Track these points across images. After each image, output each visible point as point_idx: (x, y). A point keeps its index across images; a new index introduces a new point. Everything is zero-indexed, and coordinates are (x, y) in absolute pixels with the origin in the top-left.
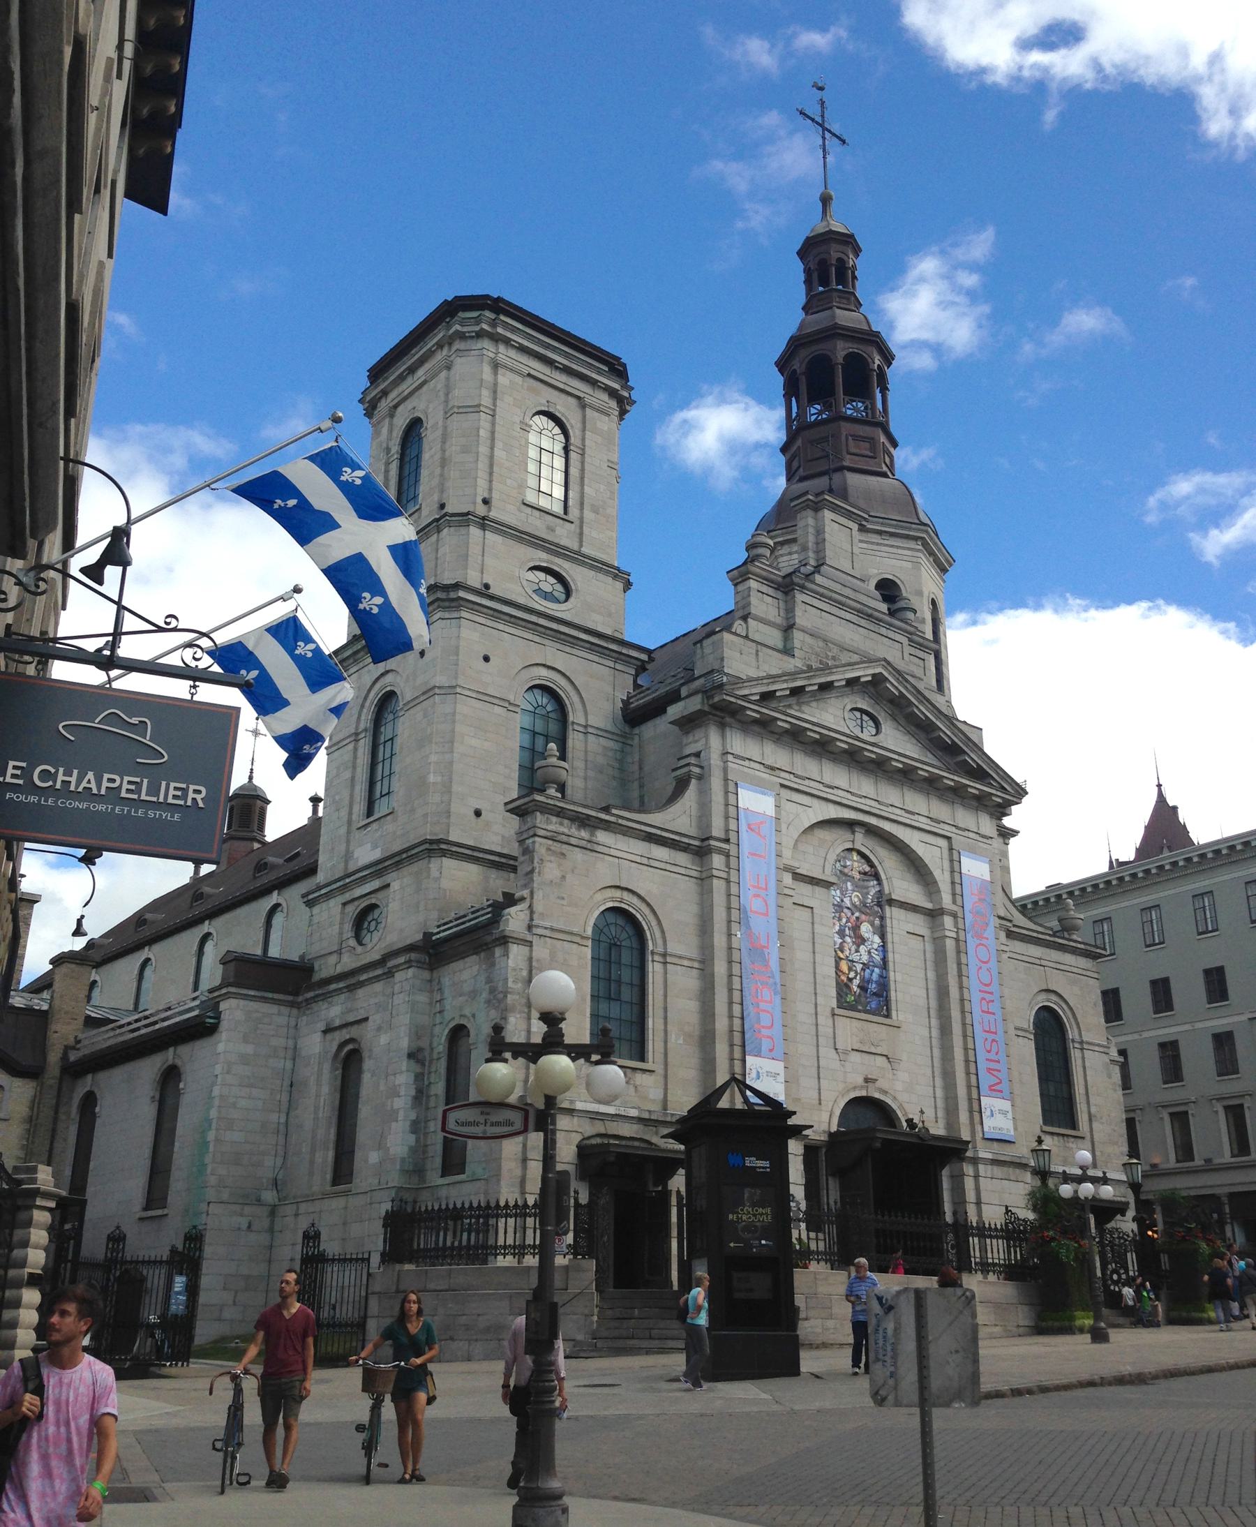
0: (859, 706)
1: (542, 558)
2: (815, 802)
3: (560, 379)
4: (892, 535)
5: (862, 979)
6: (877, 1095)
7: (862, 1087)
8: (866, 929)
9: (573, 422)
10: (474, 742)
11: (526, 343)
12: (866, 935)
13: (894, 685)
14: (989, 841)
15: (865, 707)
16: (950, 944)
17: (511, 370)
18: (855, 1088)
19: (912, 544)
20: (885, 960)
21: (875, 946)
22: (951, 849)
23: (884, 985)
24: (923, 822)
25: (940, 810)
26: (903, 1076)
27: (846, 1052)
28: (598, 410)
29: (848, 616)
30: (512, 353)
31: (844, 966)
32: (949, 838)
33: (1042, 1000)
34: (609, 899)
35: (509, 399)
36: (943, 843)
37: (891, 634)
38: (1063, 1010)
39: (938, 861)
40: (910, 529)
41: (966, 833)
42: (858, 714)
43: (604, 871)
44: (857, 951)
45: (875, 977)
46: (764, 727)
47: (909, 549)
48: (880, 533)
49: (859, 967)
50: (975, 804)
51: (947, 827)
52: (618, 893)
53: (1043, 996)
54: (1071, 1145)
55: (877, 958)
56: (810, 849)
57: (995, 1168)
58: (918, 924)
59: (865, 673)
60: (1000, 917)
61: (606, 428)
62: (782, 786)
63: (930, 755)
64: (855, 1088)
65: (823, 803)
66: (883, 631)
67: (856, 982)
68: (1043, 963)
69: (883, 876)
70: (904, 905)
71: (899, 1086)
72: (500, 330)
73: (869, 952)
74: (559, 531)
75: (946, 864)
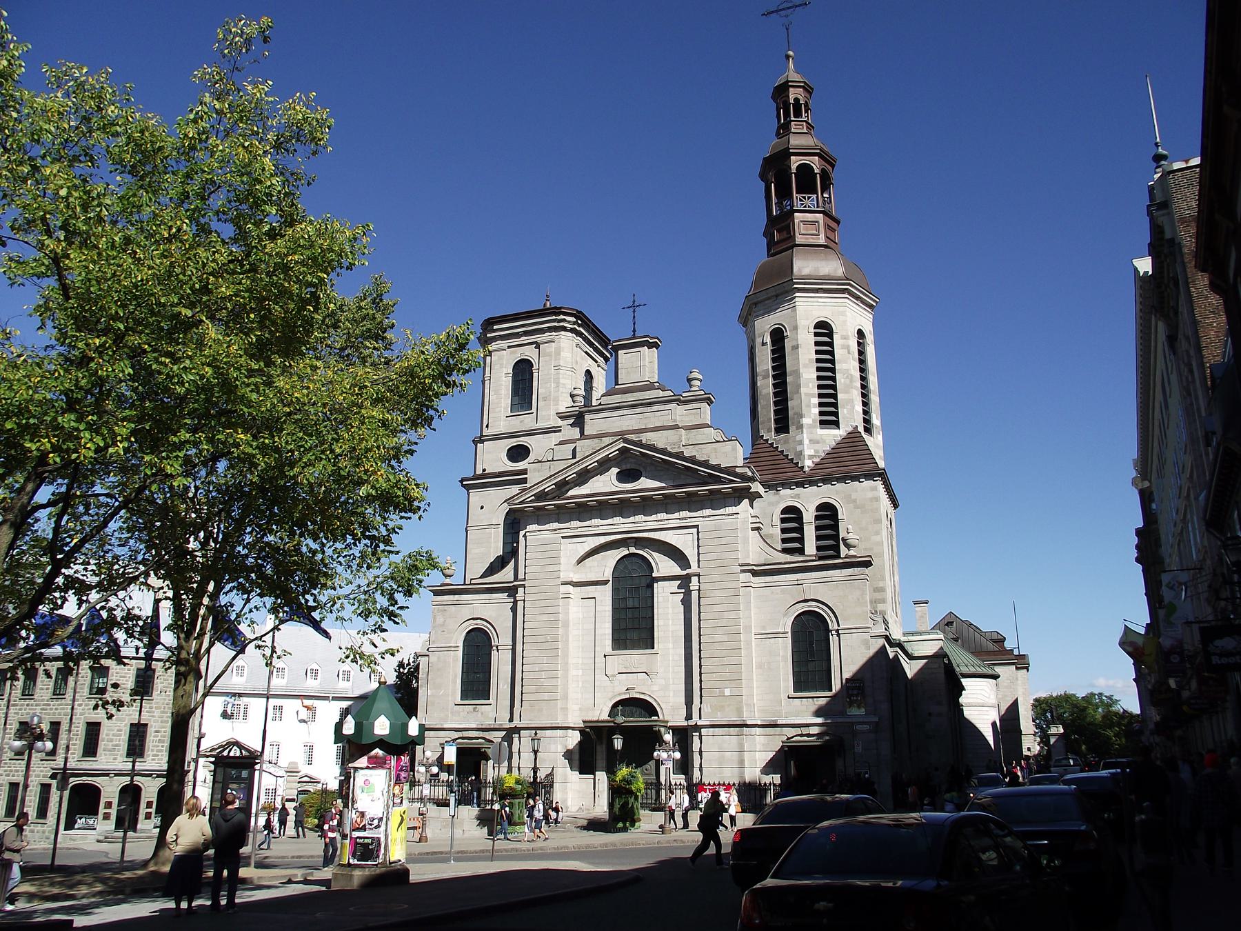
1: (513, 442)
10: (476, 551)
15: (628, 467)
16: (694, 595)
18: (619, 694)
22: (698, 532)
27: (614, 676)
32: (697, 527)
33: (803, 608)
34: (470, 625)
37: (662, 407)
39: (690, 543)
43: (466, 612)
46: (541, 516)
48: (769, 299)
50: (722, 496)
52: (475, 621)
56: (595, 564)
59: (612, 451)
62: (563, 537)
63: (683, 476)
64: (619, 694)
66: (655, 408)
68: (799, 582)
71: (655, 688)
74: (526, 421)
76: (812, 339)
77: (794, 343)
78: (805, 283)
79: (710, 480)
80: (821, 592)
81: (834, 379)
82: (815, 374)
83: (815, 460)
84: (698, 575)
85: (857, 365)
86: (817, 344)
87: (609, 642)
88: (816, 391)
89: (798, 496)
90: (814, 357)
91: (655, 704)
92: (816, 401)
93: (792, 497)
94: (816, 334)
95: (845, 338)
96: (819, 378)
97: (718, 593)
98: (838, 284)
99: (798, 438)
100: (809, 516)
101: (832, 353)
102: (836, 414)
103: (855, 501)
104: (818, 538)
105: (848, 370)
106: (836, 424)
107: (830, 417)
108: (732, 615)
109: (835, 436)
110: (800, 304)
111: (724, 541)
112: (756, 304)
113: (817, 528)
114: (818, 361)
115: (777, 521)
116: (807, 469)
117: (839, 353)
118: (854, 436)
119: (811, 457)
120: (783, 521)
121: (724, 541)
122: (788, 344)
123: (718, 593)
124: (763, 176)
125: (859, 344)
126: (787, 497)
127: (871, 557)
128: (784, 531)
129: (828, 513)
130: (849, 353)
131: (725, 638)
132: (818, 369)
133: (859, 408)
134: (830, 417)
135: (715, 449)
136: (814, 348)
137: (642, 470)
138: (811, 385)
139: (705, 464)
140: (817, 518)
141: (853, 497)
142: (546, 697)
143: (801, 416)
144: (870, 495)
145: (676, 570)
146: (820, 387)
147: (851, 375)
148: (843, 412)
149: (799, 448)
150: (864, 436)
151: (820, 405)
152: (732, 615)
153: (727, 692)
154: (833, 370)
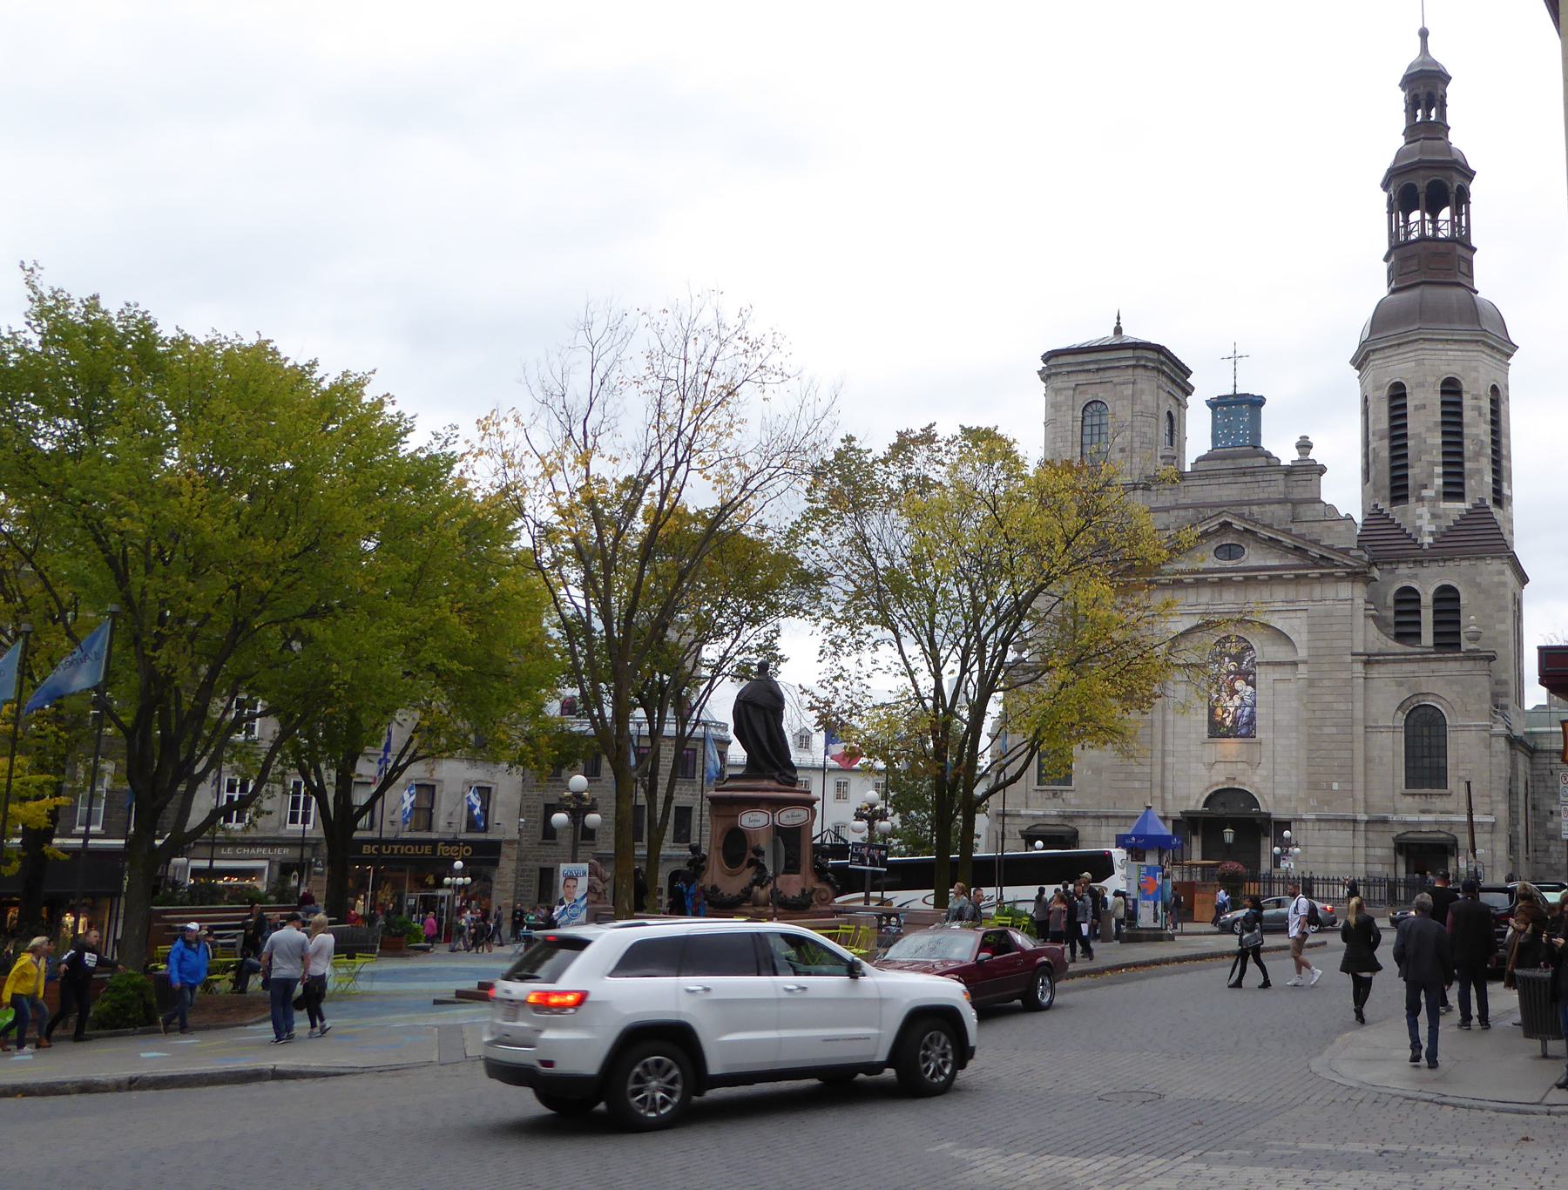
0: (1224, 543)
2: (1185, 618)
3: (1096, 378)
4: (1399, 345)
5: (1234, 718)
6: (1236, 787)
7: (1223, 783)
8: (1239, 685)
9: (1110, 399)
11: (1070, 369)
12: (1239, 689)
13: (1238, 524)
14: (1349, 602)
15: (1229, 542)
17: (1065, 389)
18: (1217, 785)
19: (1416, 346)
20: (1255, 701)
21: (1248, 693)
23: (1252, 718)
24: (1278, 606)
25: (1291, 591)
26: (1262, 772)
28: (1123, 384)
29: (1226, 481)
30: (1066, 378)
31: (1219, 711)
35: (1064, 408)
36: (1303, 614)
37: (1268, 478)
38: (1441, 704)
40: (1408, 336)
41: (1323, 603)
42: (1227, 548)
44: (1231, 699)
45: (1245, 713)
47: (1411, 351)
48: (1391, 346)
49: (1232, 710)
51: (1302, 603)
53: (1421, 698)
54: (1434, 800)
55: (1249, 701)
57: (1323, 824)
58: (1286, 672)
59: (1213, 525)
60: (1353, 654)
61: (1130, 392)
64: (1217, 785)
65: (1192, 617)
66: (1259, 478)
67: (1228, 720)
69: (1255, 647)
70: (1268, 663)
71: (1256, 779)
72: (1053, 371)
73: (1242, 699)
75: (1304, 629)
76: (1437, 399)
77: (1417, 403)
78: (1433, 334)
79: (1321, 563)
80: (1437, 687)
81: (1461, 444)
82: (1440, 441)
83: (1436, 536)
84: (1305, 662)
85: (1488, 428)
86: (1443, 403)
87: (1206, 729)
88: (1440, 459)
89: (1415, 576)
90: (1439, 418)
91: (1210, 791)
92: (1439, 470)
93: (1408, 577)
94: (1443, 392)
95: (1476, 398)
96: (1444, 443)
97: (1326, 683)
98: (1471, 335)
99: (1419, 511)
100: (1427, 599)
101: (1460, 414)
102: (1461, 485)
103: (1480, 584)
104: (1436, 623)
105: (1478, 435)
106: (1460, 496)
107: (1454, 490)
108: (1342, 707)
109: (1459, 510)
110: (1428, 357)
111: (1335, 628)
112: (1374, 351)
113: (1435, 612)
114: (1444, 423)
115: (1390, 601)
116: (1425, 547)
117: (1468, 415)
118: (1480, 510)
119: (1432, 533)
120: (1397, 602)
121: (1335, 628)
122: (1411, 402)
123: (1326, 683)
124: (1385, 185)
125: (1492, 401)
126: (1404, 576)
127: (1494, 652)
128: (1398, 613)
129: (1447, 599)
130: (1480, 415)
131: (1334, 730)
132: (1444, 433)
133: (1489, 478)
134: (1454, 490)
135: (1328, 527)
136: (1438, 409)
137: (1243, 545)
138: (1435, 452)
139: (1316, 543)
140: (1436, 600)
141: (1478, 580)
142: (1137, 785)
143: (1425, 487)
144: (1496, 579)
145: (1282, 653)
146: (1444, 453)
147: (1482, 441)
148: (1470, 484)
149: (1418, 523)
150: (1492, 509)
151: (1445, 474)
152: (1342, 707)
153: (1335, 786)
154: (1460, 434)
